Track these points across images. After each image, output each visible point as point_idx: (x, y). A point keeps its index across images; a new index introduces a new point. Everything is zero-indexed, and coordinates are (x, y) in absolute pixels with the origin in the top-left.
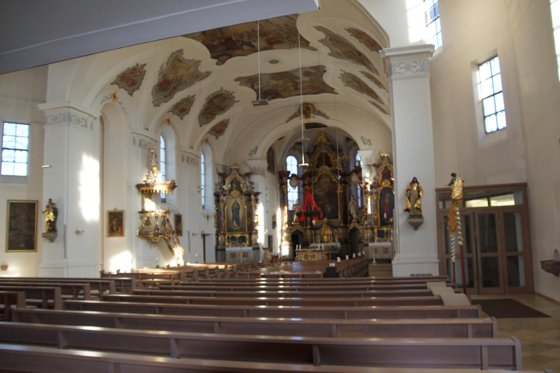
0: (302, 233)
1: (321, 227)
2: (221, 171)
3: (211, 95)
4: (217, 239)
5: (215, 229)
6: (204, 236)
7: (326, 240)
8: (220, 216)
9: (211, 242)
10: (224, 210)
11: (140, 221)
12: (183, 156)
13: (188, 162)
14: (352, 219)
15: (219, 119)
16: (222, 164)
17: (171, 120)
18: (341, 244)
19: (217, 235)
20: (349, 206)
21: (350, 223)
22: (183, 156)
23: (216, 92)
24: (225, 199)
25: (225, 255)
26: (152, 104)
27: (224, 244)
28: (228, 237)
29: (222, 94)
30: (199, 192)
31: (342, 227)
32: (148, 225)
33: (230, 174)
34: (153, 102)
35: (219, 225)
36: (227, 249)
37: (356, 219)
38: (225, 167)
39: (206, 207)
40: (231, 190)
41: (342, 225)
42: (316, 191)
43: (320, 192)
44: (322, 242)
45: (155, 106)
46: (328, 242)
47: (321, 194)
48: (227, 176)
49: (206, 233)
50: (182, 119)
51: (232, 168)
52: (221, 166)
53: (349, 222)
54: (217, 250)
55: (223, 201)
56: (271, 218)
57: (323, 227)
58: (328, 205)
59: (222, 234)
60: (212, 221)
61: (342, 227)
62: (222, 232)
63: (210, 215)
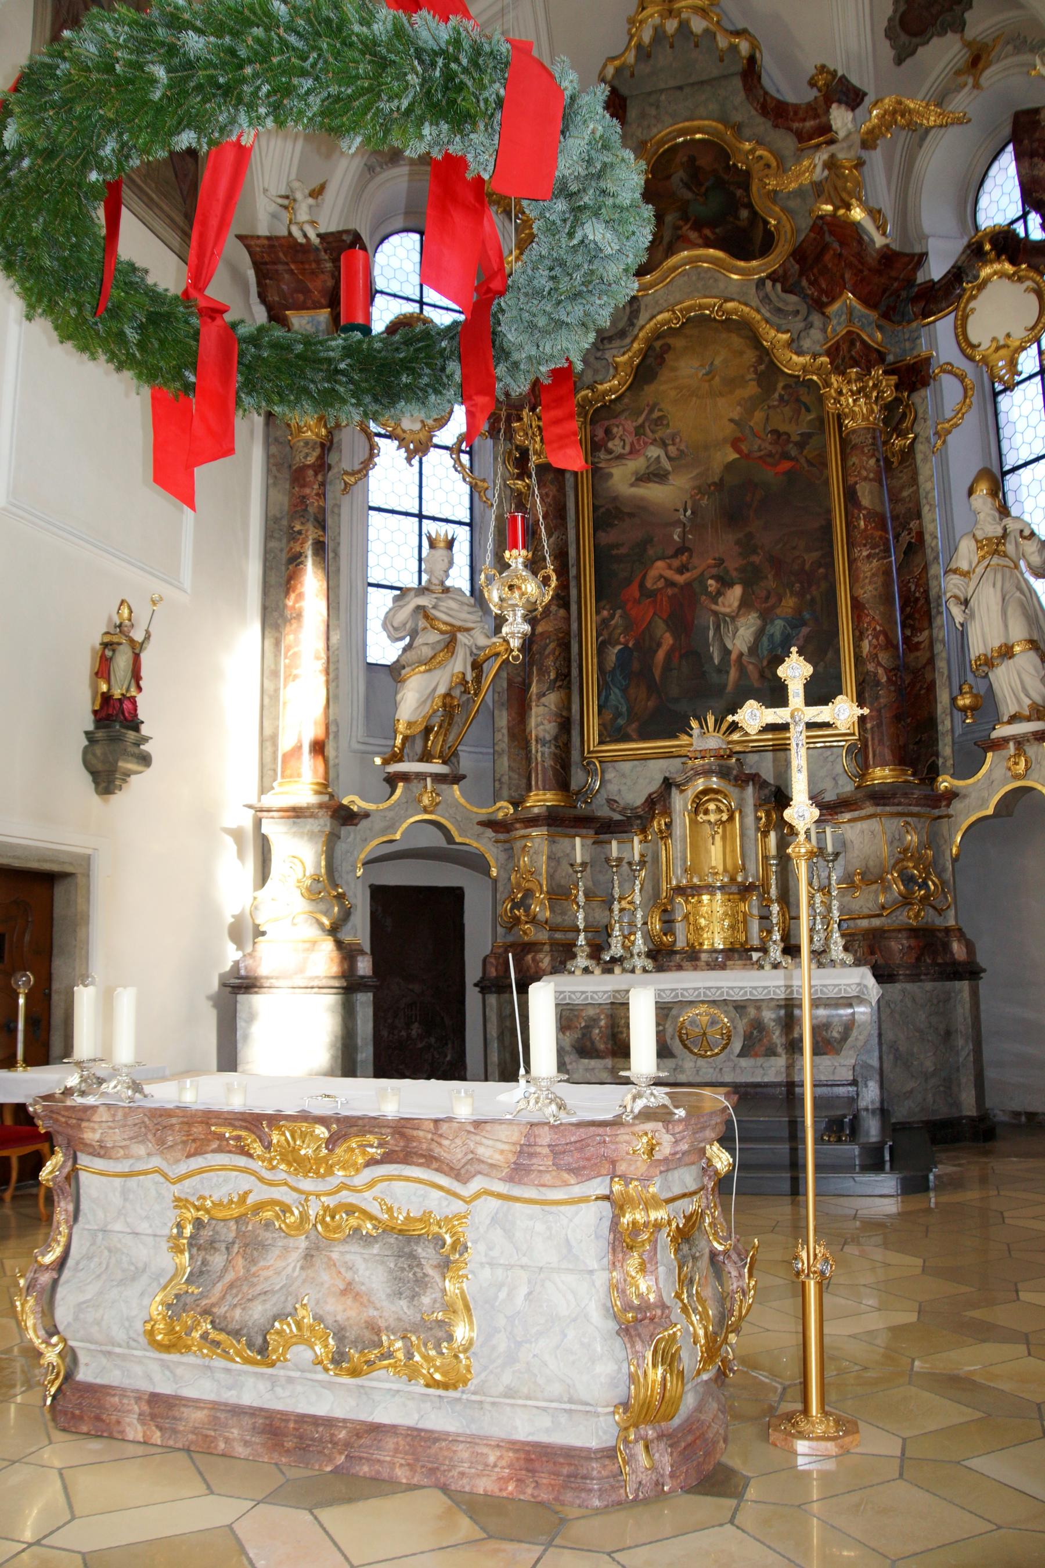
0: (477, 863)
1: (657, 804)
7: (716, 938)
14: (986, 706)
18: (882, 976)
20: (952, 585)
21: (968, 766)
31: (880, 797)
37: (1040, 712)
41: (882, 775)
42: (621, 478)
43: (655, 475)
44: (662, 956)
46: (738, 953)
47: (655, 493)
53: (946, 749)
56: (84, 665)
57: (680, 803)
58: (736, 592)
61: (880, 797)
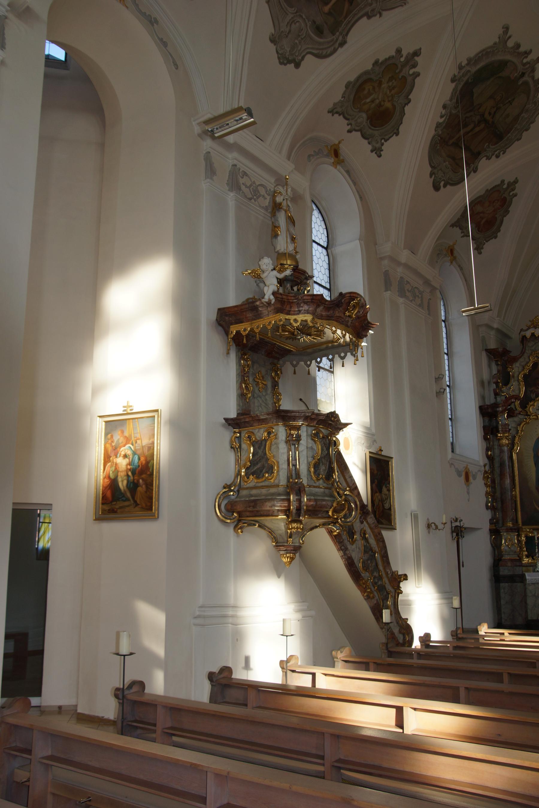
2: (492, 345)
3: (470, 61)
4: (496, 546)
5: (488, 515)
6: (458, 532)
8: (502, 475)
9: (479, 549)
10: (511, 457)
11: (231, 457)
12: (386, 274)
13: (402, 293)
15: (490, 172)
16: (495, 326)
17: (344, 150)
19: (495, 533)
22: (386, 274)
23: (485, 53)
24: (512, 423)
25: (525, 596)
26: (272, 47)
27: (520, 559)
28: (530, 540)
29: (504, 64)
30: (440, 393)
32: (258, 474)
33: (523, 353)
34: (273, 40)
35: (497, 502)
36: (530, 577)
38: (503, 335)
39: (458, 450)
40: (525, 403)
45: (284, 60)
48: (515, 359)
49: (466, 523)
50: (378, 151)
51: (528, 334)
52: (493, 333)
54: (497, 578)
55: (506, 429)
59: (510, 530)
60: (479, 488)
62: (510, 524)
63: (473, 469)
